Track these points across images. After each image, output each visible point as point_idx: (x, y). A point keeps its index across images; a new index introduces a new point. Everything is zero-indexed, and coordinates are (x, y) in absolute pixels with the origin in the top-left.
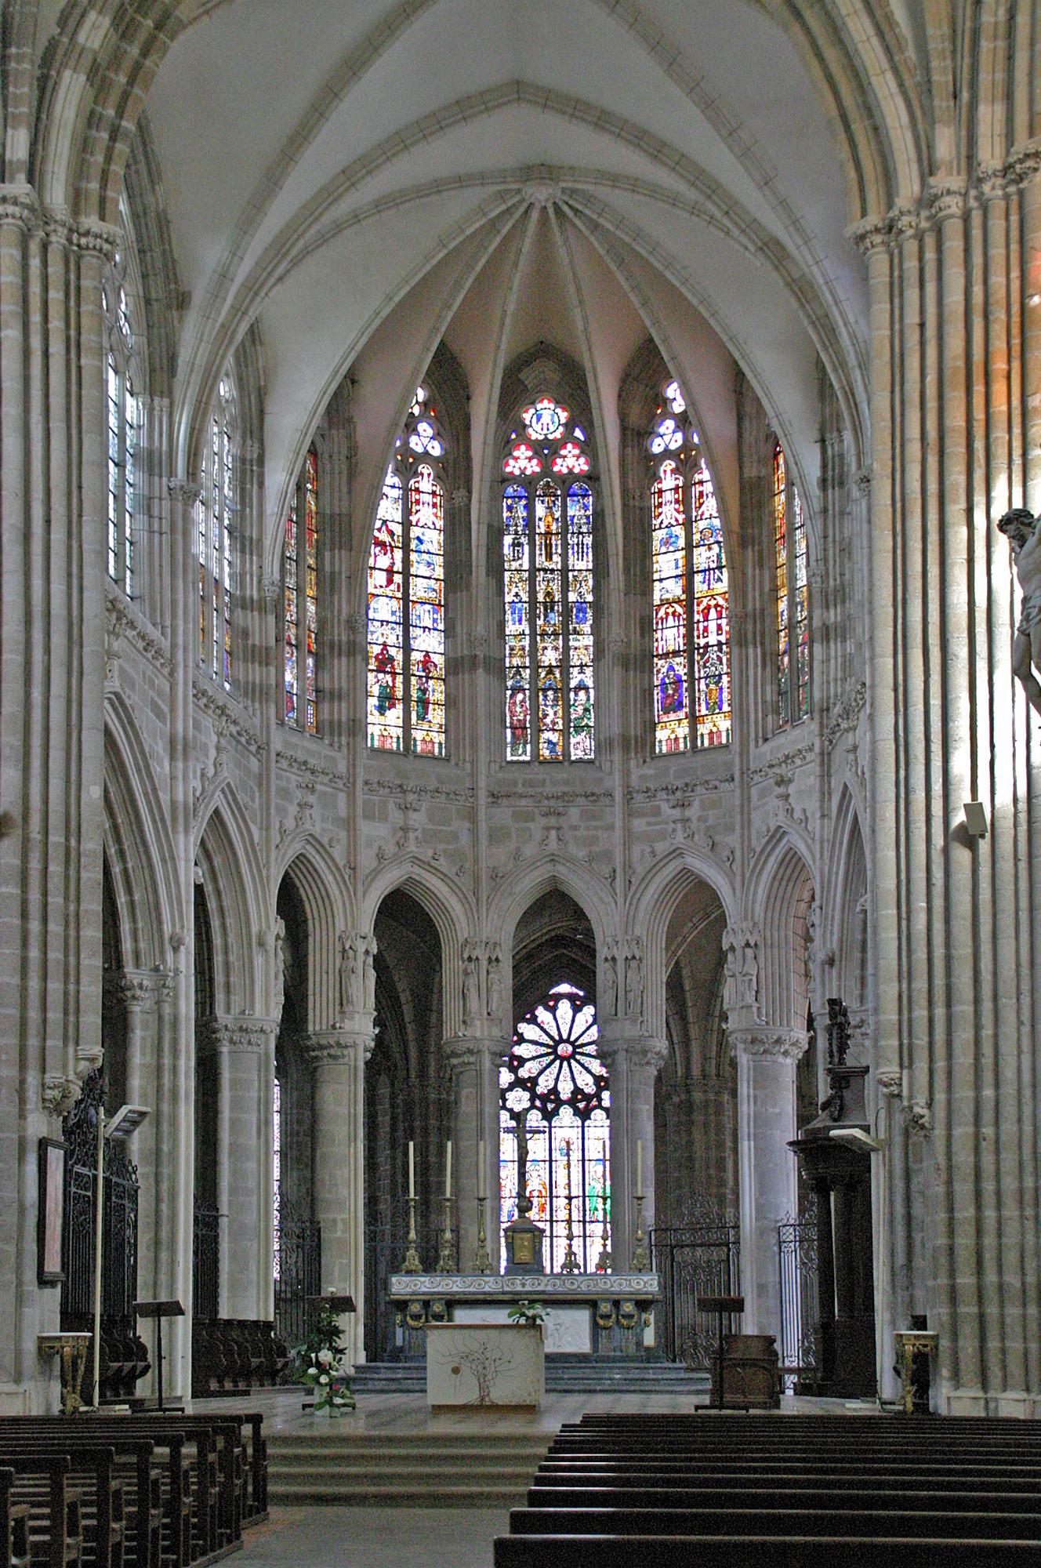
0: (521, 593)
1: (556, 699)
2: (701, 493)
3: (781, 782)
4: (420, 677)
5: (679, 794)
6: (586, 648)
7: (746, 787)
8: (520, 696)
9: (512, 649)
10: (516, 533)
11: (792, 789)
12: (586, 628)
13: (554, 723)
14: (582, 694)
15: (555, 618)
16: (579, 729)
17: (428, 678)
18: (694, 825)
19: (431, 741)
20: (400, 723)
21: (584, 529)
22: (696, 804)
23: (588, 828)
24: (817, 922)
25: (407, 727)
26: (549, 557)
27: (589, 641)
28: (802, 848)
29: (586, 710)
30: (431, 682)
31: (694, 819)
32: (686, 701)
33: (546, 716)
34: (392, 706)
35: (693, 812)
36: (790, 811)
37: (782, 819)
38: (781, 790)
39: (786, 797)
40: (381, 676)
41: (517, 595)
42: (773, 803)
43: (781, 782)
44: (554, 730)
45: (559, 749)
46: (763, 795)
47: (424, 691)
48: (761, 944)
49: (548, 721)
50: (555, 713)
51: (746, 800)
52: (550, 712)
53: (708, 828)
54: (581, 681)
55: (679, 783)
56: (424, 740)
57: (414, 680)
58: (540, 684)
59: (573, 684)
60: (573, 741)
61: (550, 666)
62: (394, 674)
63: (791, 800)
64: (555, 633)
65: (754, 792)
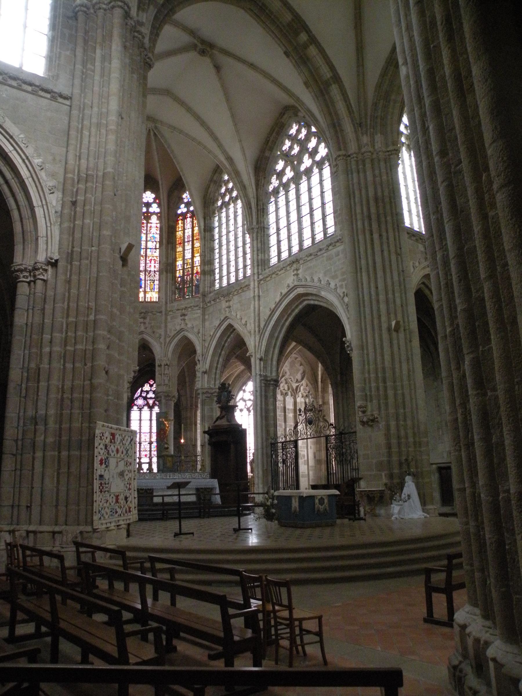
2: (151, 227)
3: (184, 315)
5: (143, 315)
7: (166, 315)
11: (186, 318)
18: (147, 325)
22: (148, 318)
24: (200, 359)
28: (192, 337)
31: (147, 323)
32: (143, 286)
35: (147, 321)
36: (187, 324)
37: (183, 326)
38: (183, 317)
39: (184, 320)
42: (179, 320)
43: (184, 315)
46: (173, 318)
51: (166, 319)
53: (151, 326)
55: (144, 311)
63: (186, 321)
65: (169, 318)
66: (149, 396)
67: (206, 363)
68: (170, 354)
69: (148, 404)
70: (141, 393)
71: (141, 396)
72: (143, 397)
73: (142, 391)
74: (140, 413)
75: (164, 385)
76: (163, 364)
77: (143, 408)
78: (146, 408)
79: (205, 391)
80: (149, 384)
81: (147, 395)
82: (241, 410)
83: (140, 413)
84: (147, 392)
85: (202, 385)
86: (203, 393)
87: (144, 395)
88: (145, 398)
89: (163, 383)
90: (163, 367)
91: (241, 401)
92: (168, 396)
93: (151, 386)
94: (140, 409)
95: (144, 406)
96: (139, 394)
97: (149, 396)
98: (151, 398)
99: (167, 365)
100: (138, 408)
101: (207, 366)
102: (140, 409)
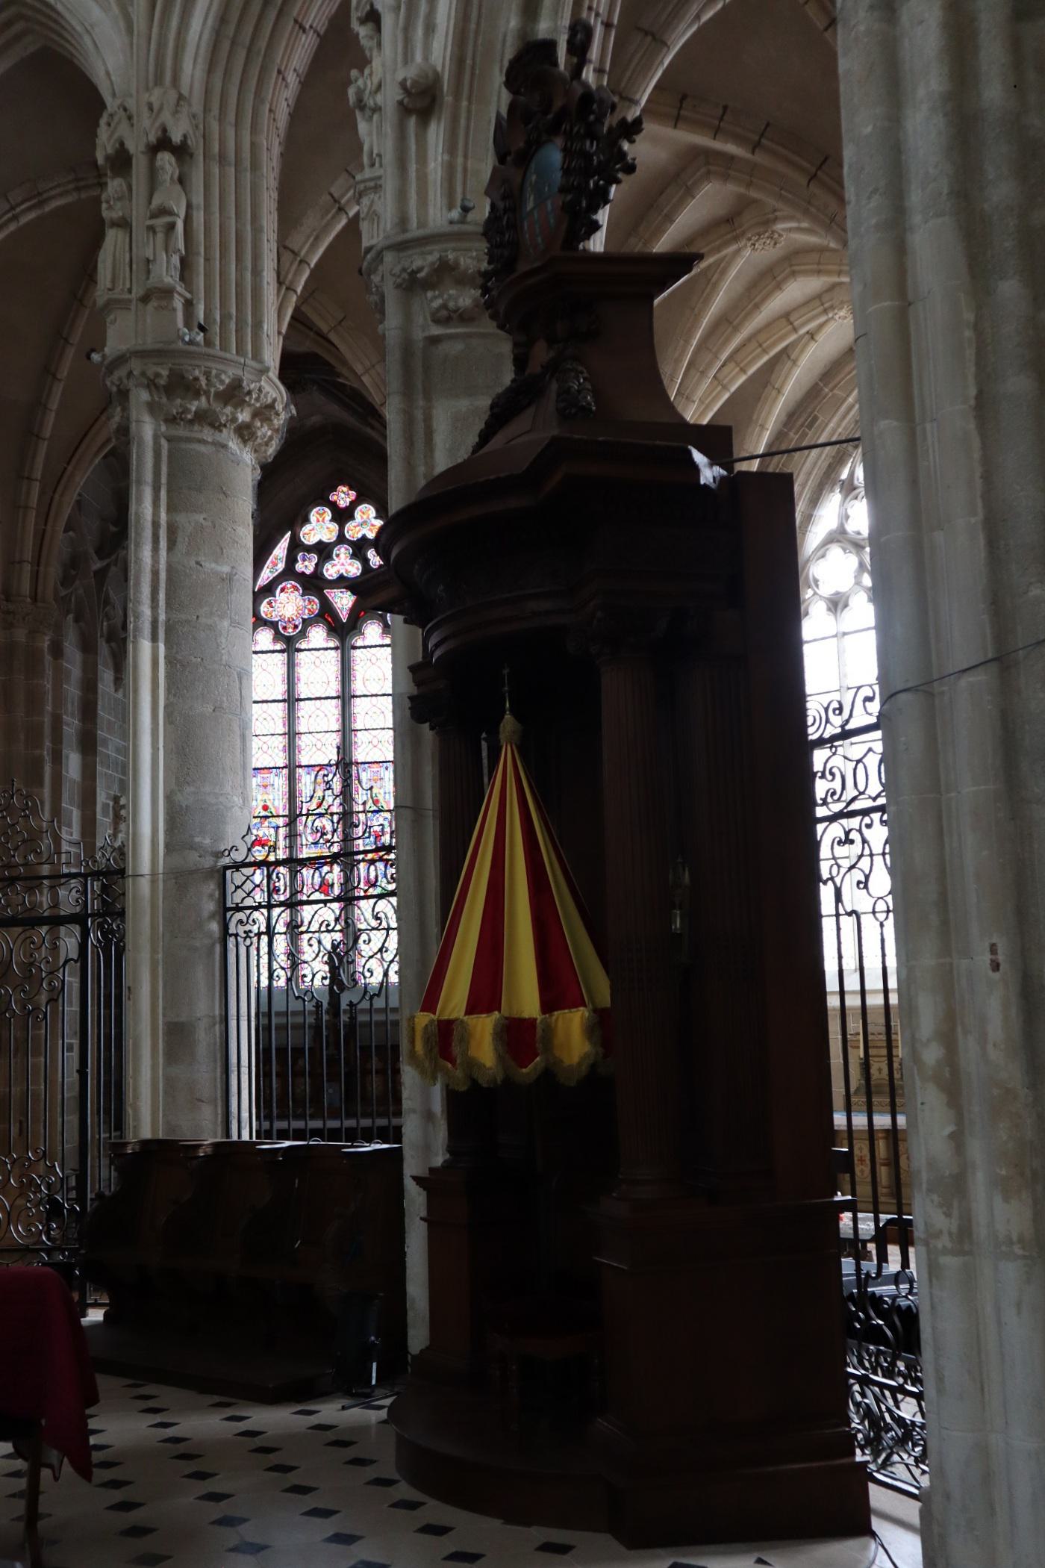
48: (196, 144)
66: (331, 571)
67: (430, 28)
68: (192, 71)
69: (326, 615)
70: (291, 560)
71: (289, 572)
72: (301, 577)
73: (296, 546)
74: (291, 666)
75: (145, 299)
76: (135, 147)
77: (303, 634)
78: (318, 635)
79: (423, 261)
80: (333, 506)
81: (319, 566)
82: (837, 604)
83: (291, 666)
84: (324, 551)
85: (403, 222)
86: (412, 285)
87: (306, 565)
88: (313, 584)
89: (138, 291)
90: (140, 165)
91: (835, 551)
92: (181, 385)
93: (342, 516)
94: (289, 644)
95: (307, 623)
96: (281, 566)
97: (331, 571)
98: (342, 582)
99: (163, 143)
100: (278, 636)
101: (439, 52)
102: (289, 644)
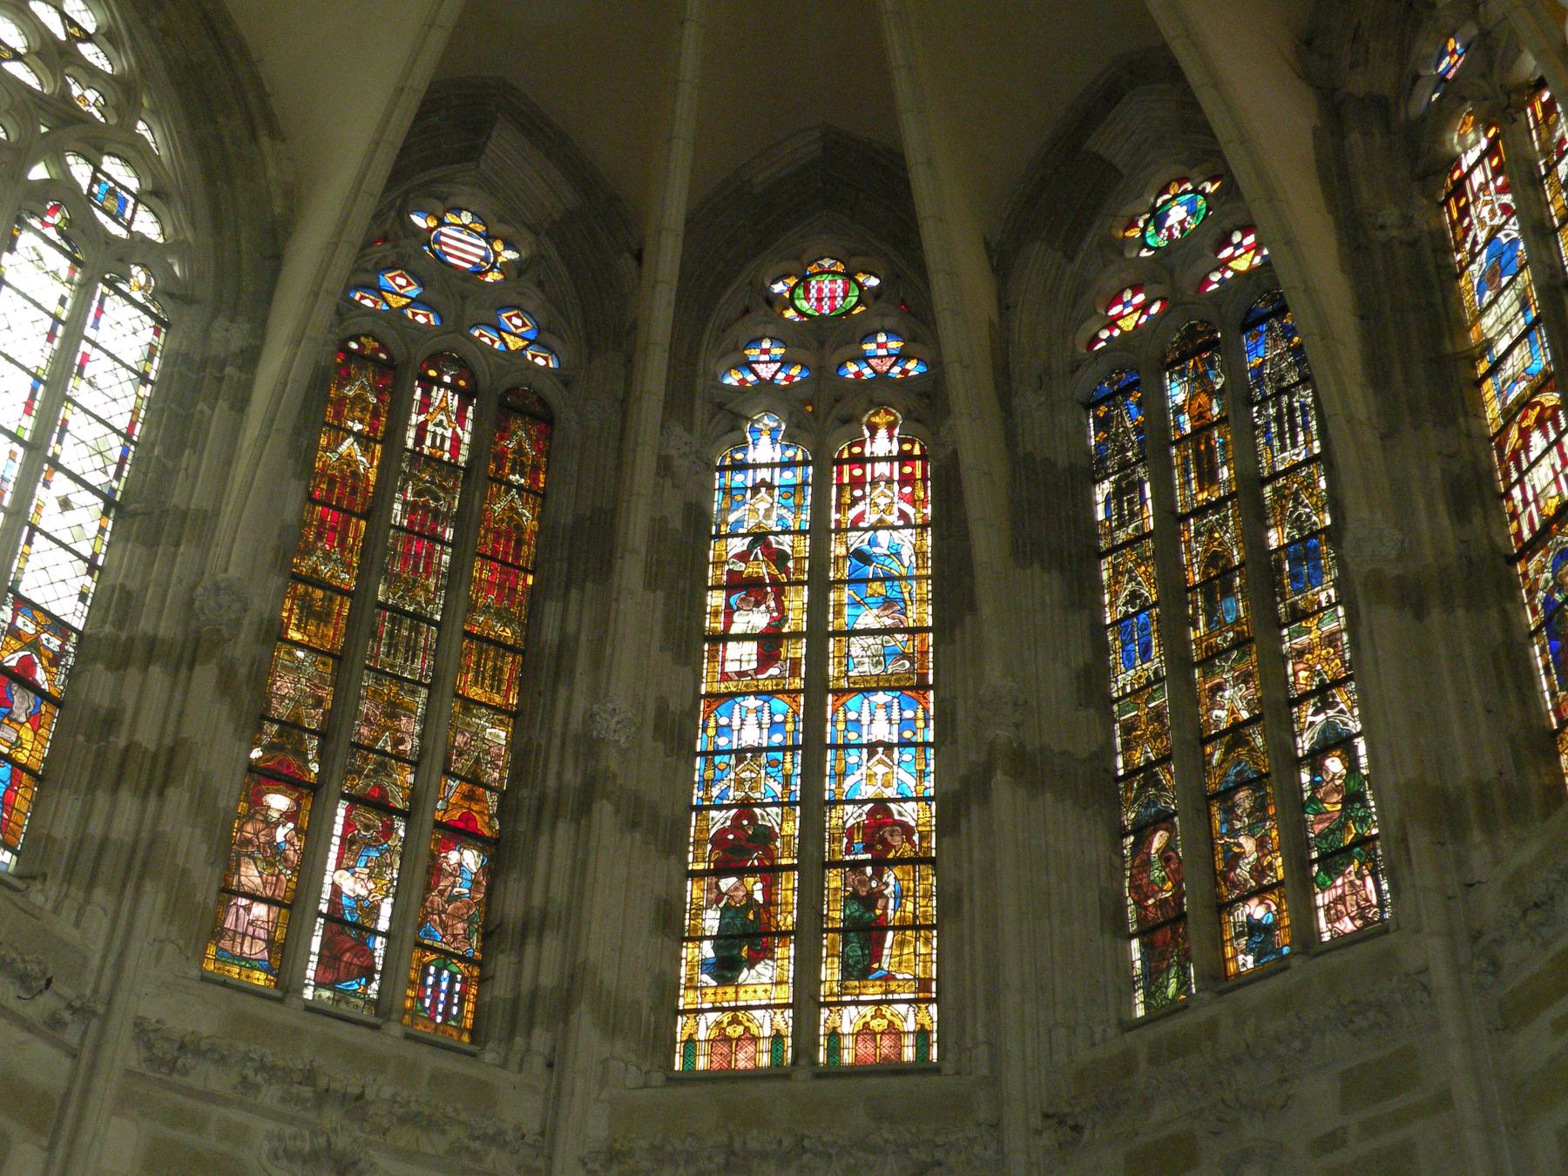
0: (1144, 591)
1: (1259, 808)
4: (857, 866)
6: (1331, 640)
8: (1158, 840)
9: (1128, 728)
10: (1125, 465)
12: (1326, 594)
13: (1259, 870)
14: (1334, 765)
15: (1236, 608)
16: (1334, 861)
17: (880, 864)
19: (894, 1032)
20: (785, 994)
21: (1292, 378)
23: (1370, 1128)
25: (806, 1002)
26: (1208, 477)
27: (1335, 622)
29: (1352, 798)
30: (890, 877)
33: (1234, 859)
34: (762, 953)
40: (727, 883)
41: (1134, 596)
44: (1260, 892)
45: (1283, 938)
47: (871, 900)
49: (1243, 871)
50: (1261, 845)
52: (1248, 844)
54: (1329, 724)
56: (865, 1032)
57: (834, 880)
58: (1213, 784)
59: (1304, 744)
60: (1321, 899)
61: (1237, 727)
62: (770, 873)
64: (1241, 643)
